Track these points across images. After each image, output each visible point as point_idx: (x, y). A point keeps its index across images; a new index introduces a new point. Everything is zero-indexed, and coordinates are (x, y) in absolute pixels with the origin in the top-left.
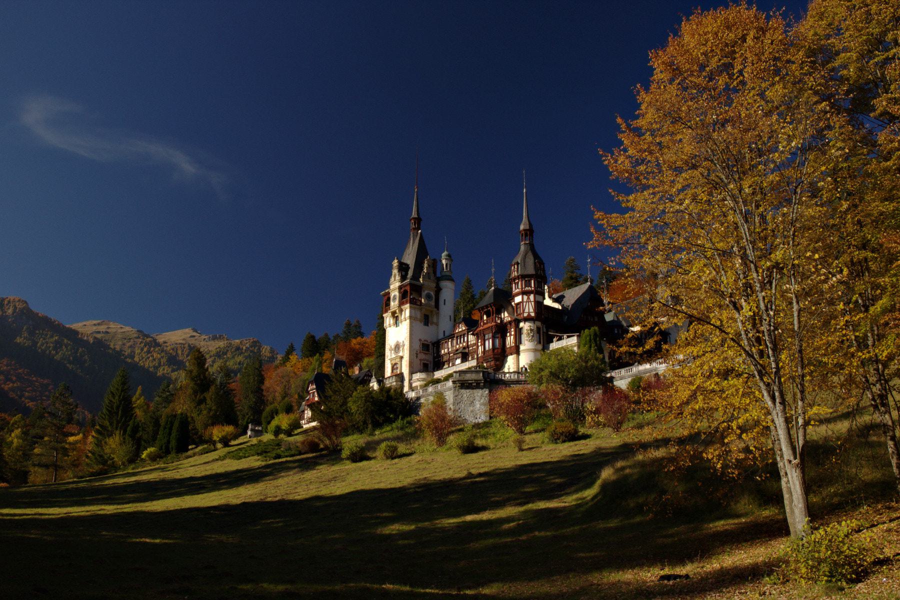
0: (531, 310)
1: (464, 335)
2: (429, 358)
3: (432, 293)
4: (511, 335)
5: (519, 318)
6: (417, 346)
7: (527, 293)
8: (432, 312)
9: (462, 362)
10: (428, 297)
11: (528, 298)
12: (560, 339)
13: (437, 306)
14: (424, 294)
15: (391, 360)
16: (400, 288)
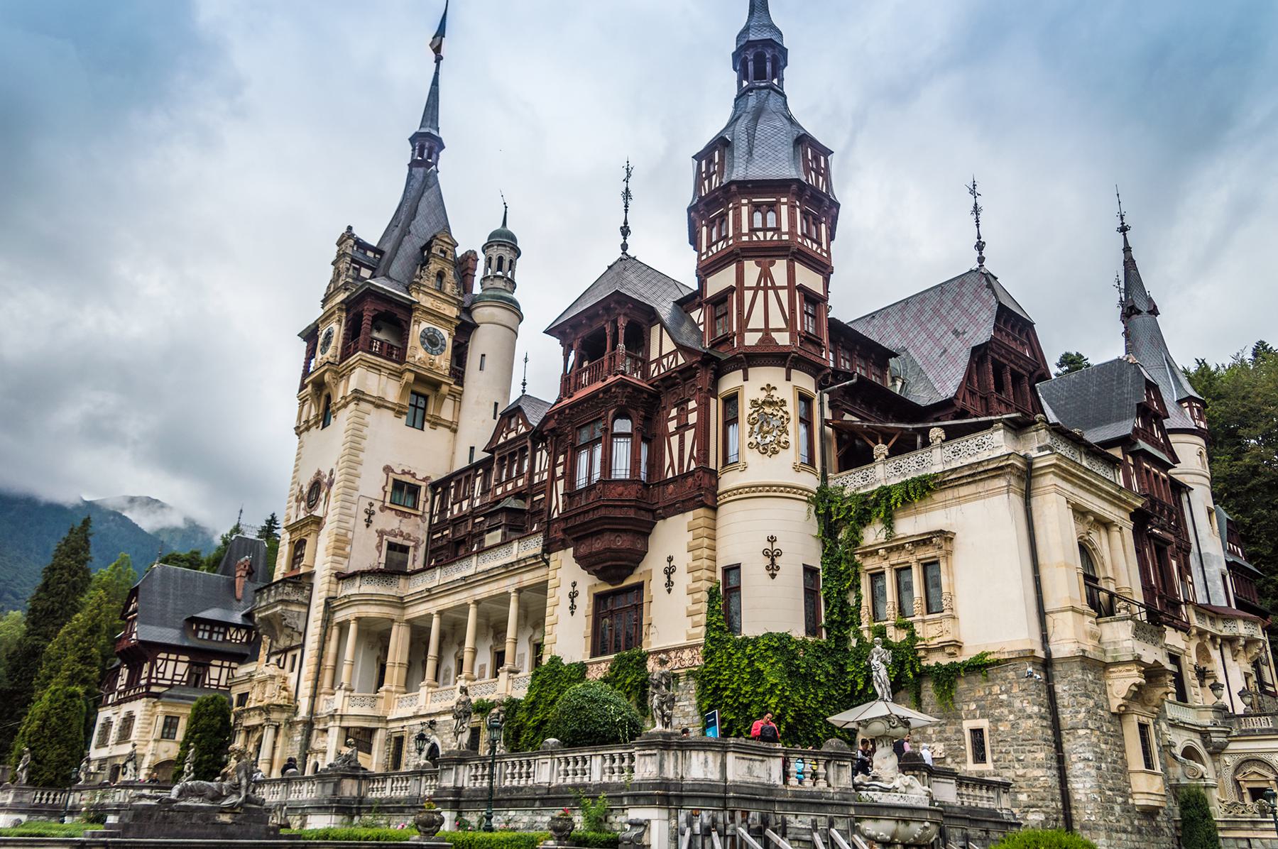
0: (777, 321)
1: (525, 449)
2: (415, 529)
3: (446, 334)
4: (683, 427)
5: (723, 354)
6: (373, 486)
7: (765, 253)
8: (436, 385)
9: (505, 542)
10: (431, 341)
11: (766, 274)
12: (902, 446)
13: (458, 371)
14: (417, 330)
15: (292, 529)
16: (347, 305)
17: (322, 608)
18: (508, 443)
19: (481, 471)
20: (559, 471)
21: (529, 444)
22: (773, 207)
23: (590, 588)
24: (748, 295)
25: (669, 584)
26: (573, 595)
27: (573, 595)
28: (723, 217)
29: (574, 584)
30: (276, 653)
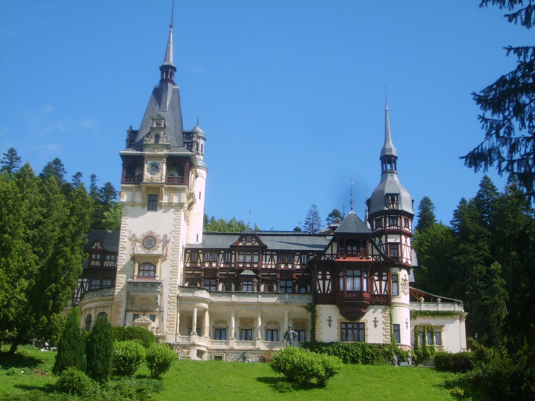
0: (409, 258)
11: (406, 241)
17: (176, 298)
18: (244, 246)
19: (222, 252)
20: (320, 277)
21: (260, 252)
22: (408, 220)
23: (338, 320)
24: (403, 246)
25: (375, 326)
26: (330, 321)
27: (330, 321)
28: (396, 218)
29: (330, 317)
30: (133, 311)
